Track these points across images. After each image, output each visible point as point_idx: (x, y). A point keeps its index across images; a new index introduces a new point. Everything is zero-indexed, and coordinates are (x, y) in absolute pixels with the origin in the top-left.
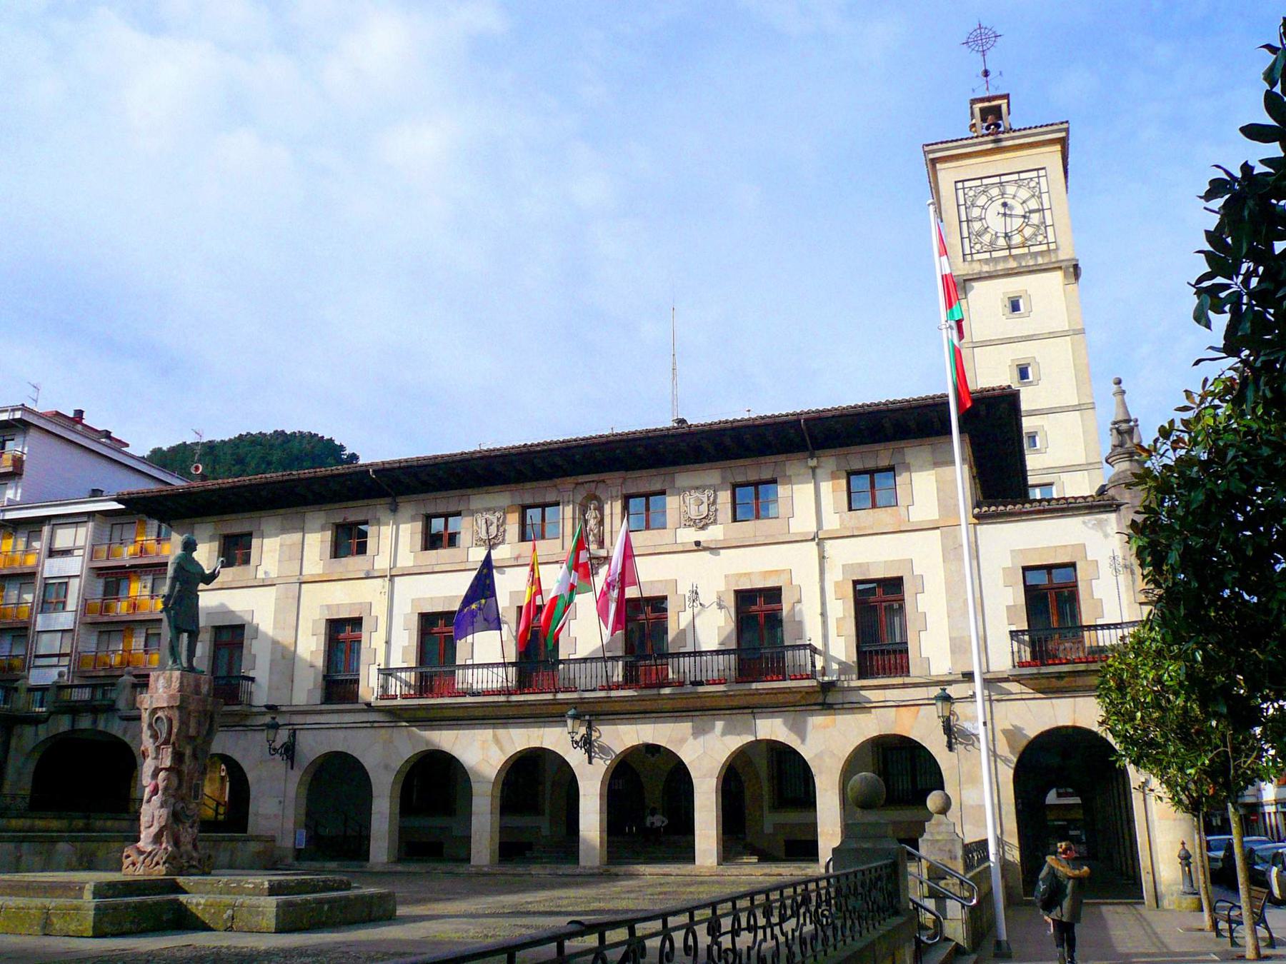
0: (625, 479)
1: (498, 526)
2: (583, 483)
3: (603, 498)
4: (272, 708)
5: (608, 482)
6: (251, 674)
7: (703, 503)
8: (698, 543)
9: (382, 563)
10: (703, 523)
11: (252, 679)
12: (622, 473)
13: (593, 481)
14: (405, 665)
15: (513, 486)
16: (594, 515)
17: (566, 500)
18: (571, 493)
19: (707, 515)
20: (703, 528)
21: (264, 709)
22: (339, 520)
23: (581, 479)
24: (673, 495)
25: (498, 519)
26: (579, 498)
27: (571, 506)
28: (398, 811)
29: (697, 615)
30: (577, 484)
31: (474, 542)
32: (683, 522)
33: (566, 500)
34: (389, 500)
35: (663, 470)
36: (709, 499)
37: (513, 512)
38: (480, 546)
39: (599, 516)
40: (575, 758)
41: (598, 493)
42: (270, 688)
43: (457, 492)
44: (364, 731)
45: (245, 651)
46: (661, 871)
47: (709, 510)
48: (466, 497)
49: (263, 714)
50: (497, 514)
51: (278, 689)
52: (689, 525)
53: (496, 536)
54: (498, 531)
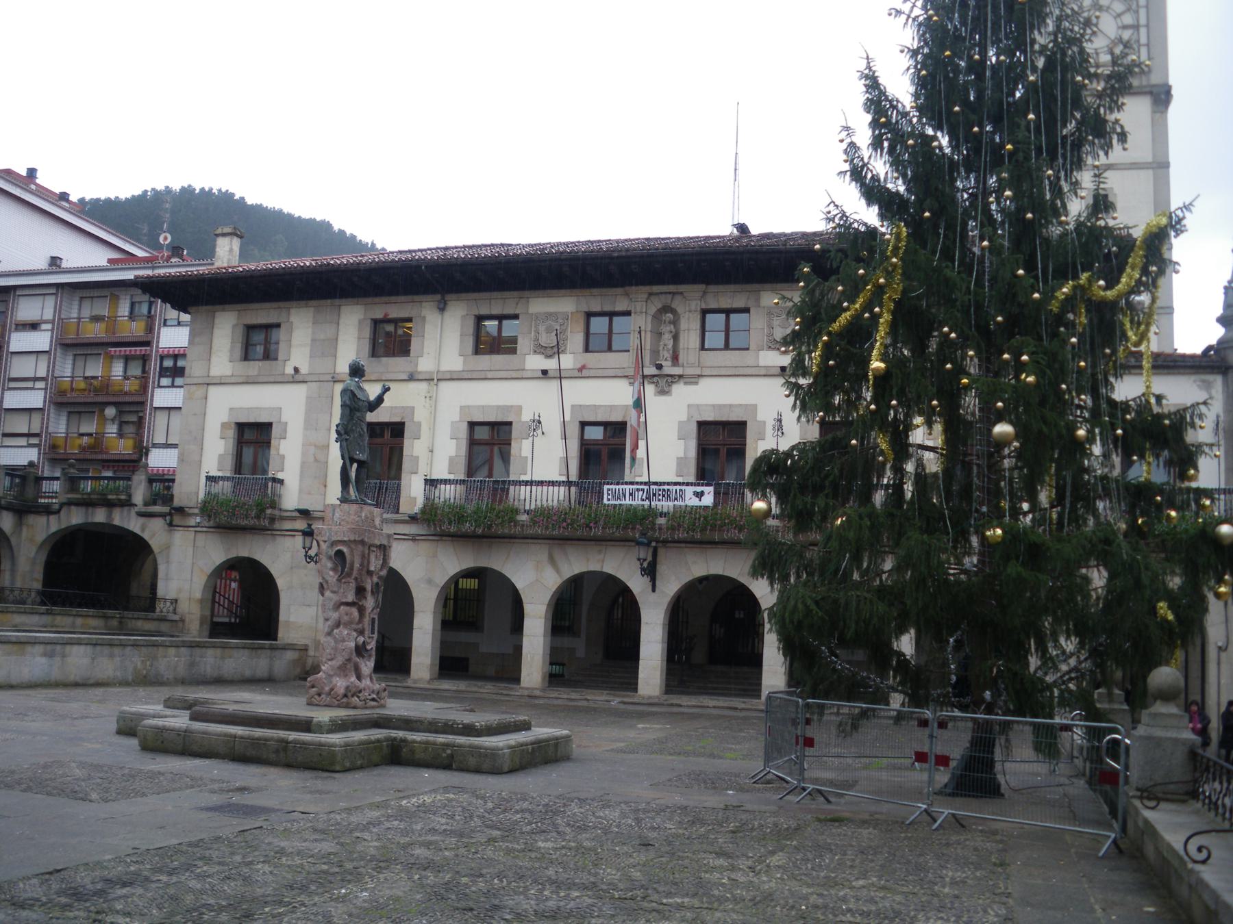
0: (705, 293)
2: (657, 294)
3: (680, 310)
4: (304, 513)
5: (685, 294)
6: (280, 476)
9: (425, 364)
11: (281, 482)
12: (703, 287)
14: (452, 477)
15: (577, 291)
21: (297, 514)
22: (379, 315)
23: (656, 289)
26: (653, 309)
28: (439, 627)
30: (651, 294)
33: (638, 309)
34: (438, 297)
35: (749, 287)
40: (637, 584)
42: (301, 491)
43: (515, 294)
44: (405, 542)
45: (273, 451)
46: (726, 704)
49: (293, 519)
51: (309, 494)
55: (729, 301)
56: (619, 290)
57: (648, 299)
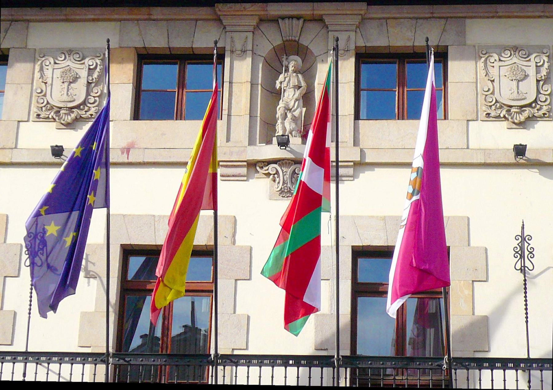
0: (364, 19)
1: (89, 83)
2: (275, 20)
3: (315, 48)
5: (327, 20)
7: (526, 76)
8: (520, 150)
10: (526, 114)
13: (298, 18)
15: (123, 12)
16: (294, 81)
17: (238, 46)
18: (250, 35)
19: (535, 101)
20: (522, 125)
23: (275, 9)
24: (462, 57)
25: (91, 71)
27: (249, 60)
29: (514, 293)
31: (34, 109)
32: (483, 109)
33: (238, 46)
36: (538, 72)
37: (122, 61)
38: (47, 119)
39: (303, 84)
41: (304, 41)
47: (538, 92)
48: (18, 25)
50: (88, 62)
52: (499, 117)
53: (84, 103)
54: (88, 94)
55: (410, 34)
56: (203, 12)
57: (257, 27)
